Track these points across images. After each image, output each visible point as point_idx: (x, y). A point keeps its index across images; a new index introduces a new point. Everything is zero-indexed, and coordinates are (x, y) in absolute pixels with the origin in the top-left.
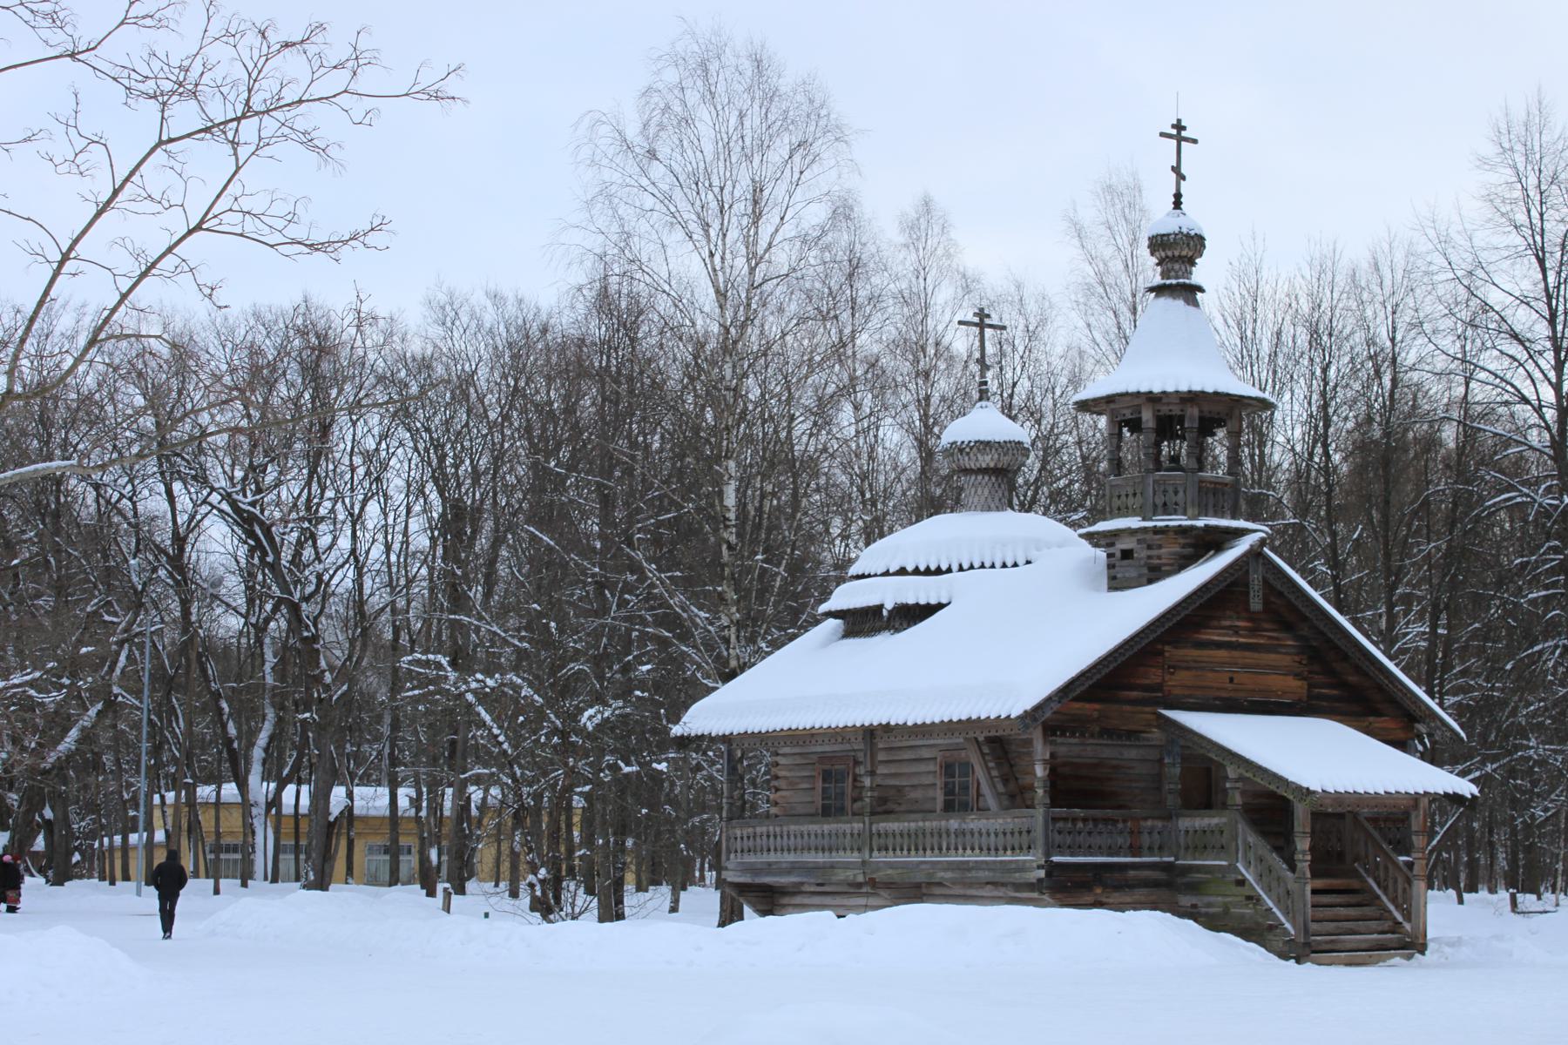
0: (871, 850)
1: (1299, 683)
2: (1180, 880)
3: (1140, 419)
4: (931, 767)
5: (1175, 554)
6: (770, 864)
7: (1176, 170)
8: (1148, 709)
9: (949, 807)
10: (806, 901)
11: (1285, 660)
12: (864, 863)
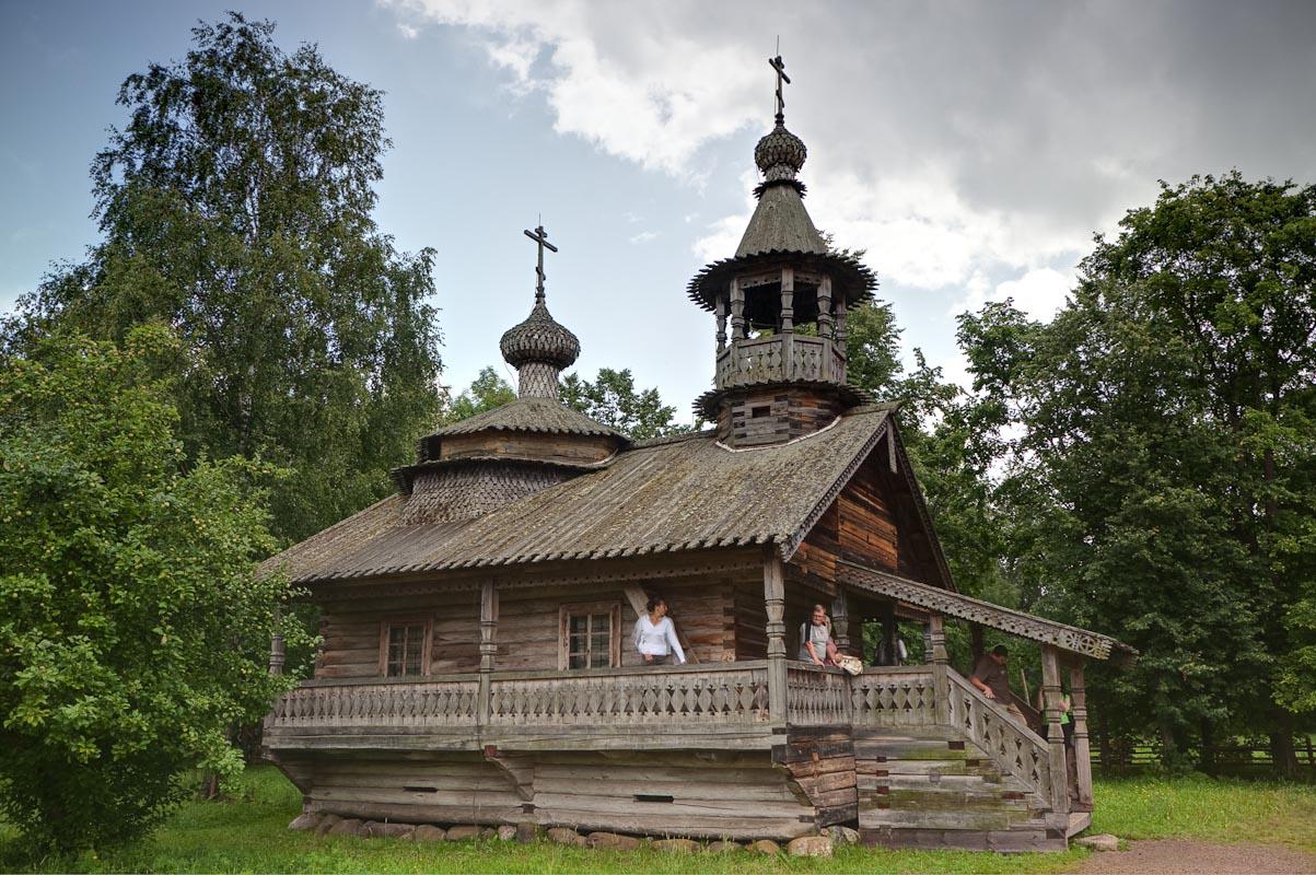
0: (491, 712)
1: (893, 551)
2: (856, 744)
3: (780, 283)
4: (549, 621)
5: (814, 412)
6: (333, 730)
7: (779, 94)
8: (832, 557)
9: (575, 663)
10: (361, 770)
11: (889, 527)
12: (479, 728)
